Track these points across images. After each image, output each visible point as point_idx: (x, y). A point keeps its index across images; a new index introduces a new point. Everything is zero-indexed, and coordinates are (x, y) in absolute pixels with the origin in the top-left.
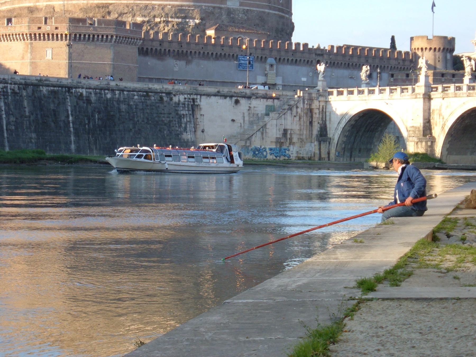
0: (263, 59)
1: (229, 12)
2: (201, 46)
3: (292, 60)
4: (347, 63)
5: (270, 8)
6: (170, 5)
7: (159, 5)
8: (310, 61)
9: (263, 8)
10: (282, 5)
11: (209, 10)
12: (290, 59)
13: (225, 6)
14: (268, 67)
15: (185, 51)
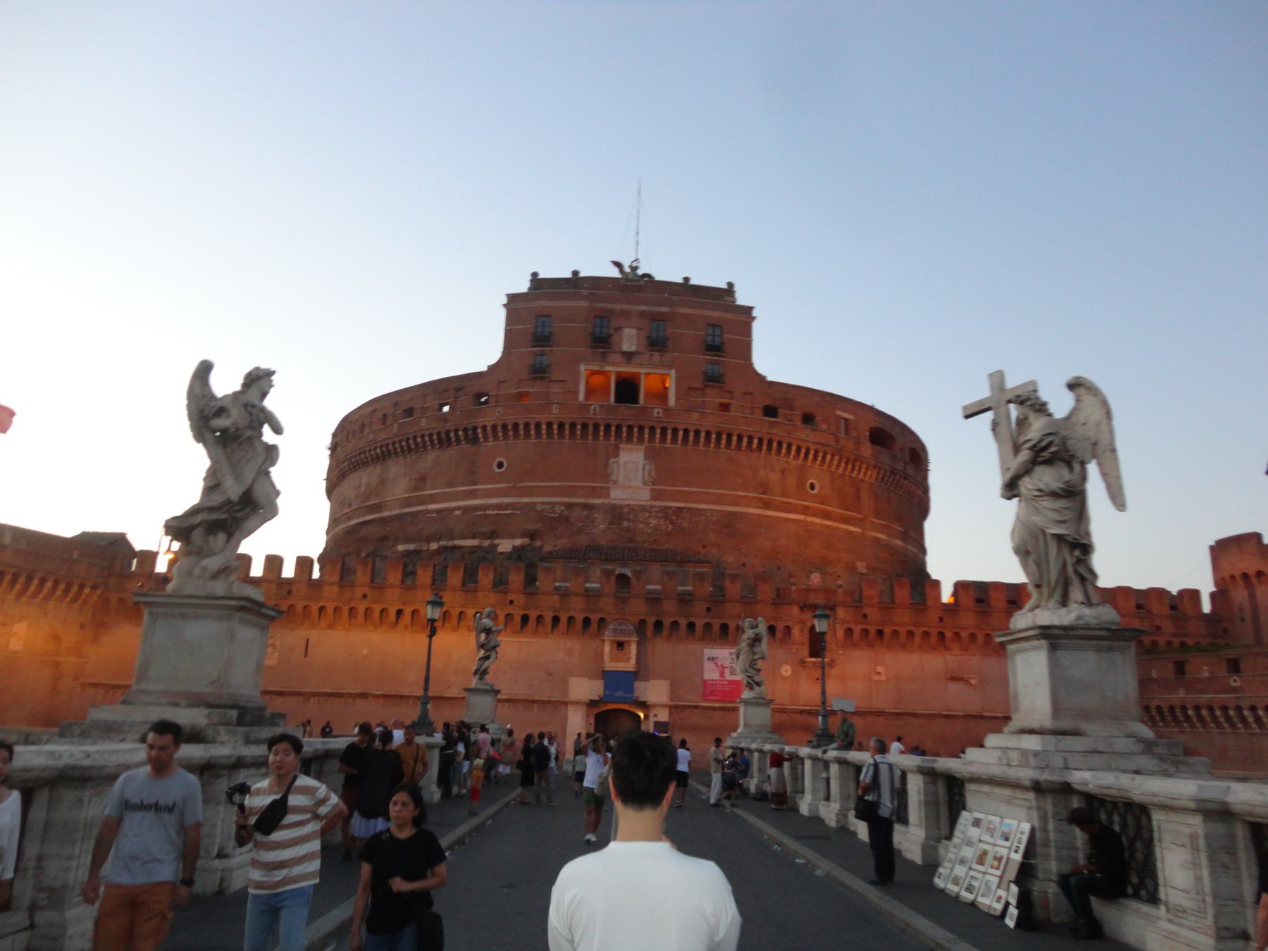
0: (594, 626)
1: (617, 514)
2: (359, 592)
3: (708, 626)
4: (934, 632)
5: (767, 505)
6: (458, 508)
7: (439, 511)
8: (780, 627)
9: (736, 504)
10: (822, 499)
11: (554, 512)
12: (699, 623)
13: (605, 501)
14: (607, 649)
15: (300, 605)
